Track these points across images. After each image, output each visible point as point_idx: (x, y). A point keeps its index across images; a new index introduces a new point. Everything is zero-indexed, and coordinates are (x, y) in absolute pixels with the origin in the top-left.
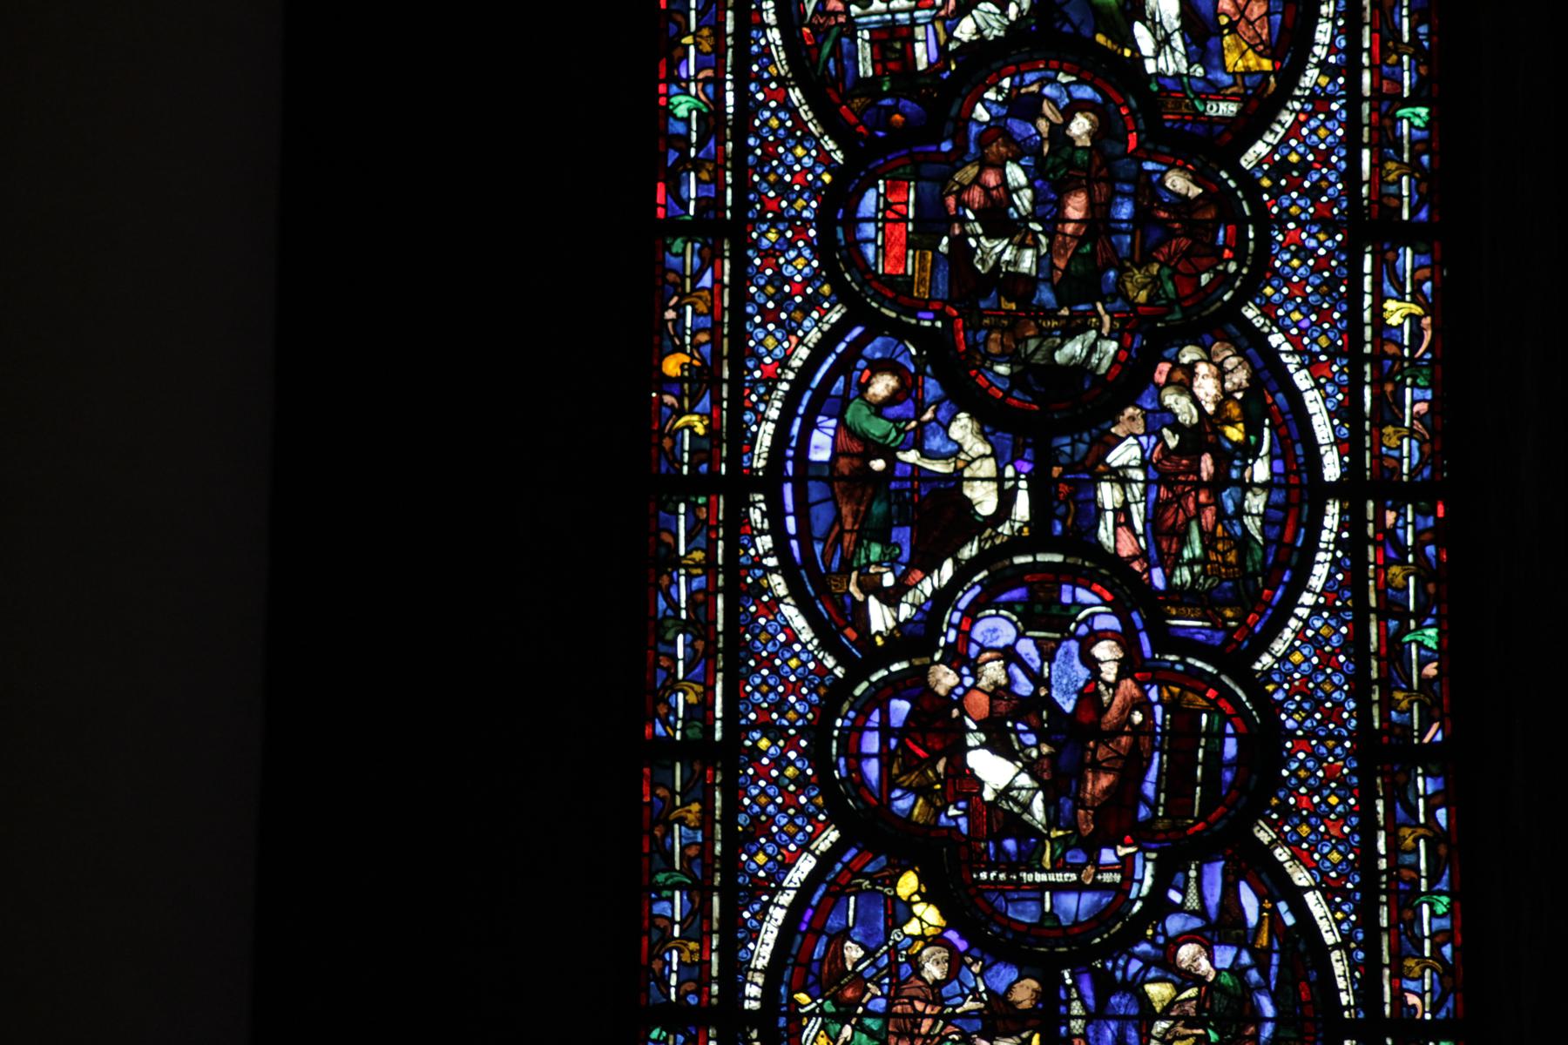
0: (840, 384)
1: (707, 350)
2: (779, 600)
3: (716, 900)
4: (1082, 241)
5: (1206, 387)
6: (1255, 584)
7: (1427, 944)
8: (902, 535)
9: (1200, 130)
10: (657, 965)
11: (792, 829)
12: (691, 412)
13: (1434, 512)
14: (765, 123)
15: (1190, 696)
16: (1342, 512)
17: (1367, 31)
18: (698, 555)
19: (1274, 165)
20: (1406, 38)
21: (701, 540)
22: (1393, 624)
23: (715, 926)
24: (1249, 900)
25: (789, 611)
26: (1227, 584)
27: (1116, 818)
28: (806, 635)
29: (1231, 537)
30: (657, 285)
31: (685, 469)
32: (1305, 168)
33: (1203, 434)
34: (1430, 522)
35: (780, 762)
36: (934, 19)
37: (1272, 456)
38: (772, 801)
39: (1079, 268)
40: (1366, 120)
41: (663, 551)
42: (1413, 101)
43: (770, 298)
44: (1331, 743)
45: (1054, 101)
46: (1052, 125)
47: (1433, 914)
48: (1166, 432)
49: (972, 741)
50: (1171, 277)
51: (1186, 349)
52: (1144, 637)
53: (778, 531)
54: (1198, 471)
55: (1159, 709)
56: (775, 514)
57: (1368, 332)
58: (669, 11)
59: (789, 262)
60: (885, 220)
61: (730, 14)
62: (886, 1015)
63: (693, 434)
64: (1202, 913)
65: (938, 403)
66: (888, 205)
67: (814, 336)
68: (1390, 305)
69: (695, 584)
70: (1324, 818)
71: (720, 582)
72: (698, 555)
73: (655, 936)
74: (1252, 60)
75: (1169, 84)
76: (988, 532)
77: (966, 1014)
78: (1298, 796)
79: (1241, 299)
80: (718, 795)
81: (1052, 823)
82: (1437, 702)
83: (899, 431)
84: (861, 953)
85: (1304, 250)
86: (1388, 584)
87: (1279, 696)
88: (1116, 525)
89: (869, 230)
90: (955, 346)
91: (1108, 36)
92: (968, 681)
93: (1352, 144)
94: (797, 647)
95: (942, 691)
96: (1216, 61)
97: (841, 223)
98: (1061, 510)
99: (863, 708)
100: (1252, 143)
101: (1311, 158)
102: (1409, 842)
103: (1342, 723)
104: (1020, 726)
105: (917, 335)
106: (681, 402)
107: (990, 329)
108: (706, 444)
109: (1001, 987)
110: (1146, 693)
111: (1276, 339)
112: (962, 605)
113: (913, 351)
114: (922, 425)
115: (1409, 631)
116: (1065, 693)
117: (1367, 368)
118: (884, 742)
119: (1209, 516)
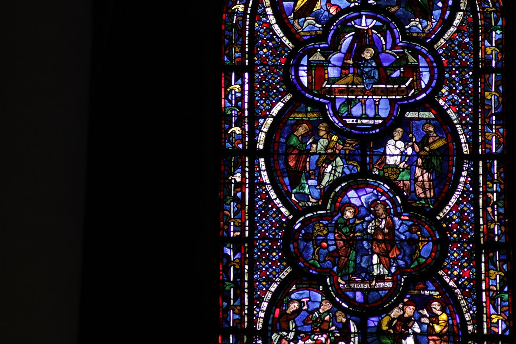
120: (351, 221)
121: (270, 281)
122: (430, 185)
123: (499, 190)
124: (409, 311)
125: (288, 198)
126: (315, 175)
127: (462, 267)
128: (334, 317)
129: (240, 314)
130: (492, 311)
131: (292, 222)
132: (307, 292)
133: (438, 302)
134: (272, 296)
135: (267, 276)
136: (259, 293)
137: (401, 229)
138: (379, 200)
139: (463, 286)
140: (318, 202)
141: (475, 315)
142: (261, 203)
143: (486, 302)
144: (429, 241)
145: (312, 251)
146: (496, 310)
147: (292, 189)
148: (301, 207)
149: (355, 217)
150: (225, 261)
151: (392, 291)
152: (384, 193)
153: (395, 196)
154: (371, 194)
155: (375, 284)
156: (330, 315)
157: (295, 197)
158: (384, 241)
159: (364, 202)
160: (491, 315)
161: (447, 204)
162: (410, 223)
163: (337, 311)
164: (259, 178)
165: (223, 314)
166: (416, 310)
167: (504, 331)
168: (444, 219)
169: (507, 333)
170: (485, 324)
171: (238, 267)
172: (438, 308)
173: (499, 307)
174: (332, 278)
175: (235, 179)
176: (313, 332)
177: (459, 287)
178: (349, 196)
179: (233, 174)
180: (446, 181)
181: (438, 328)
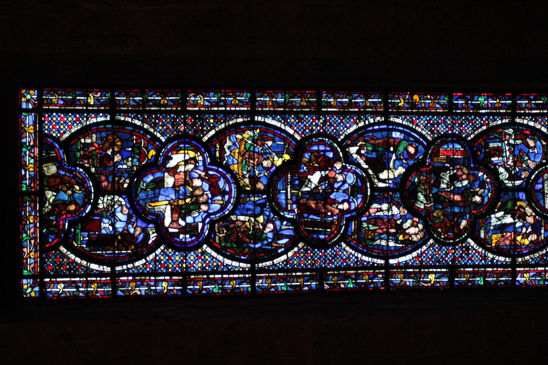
0: (412, 139)
1: (420, 106)
2: (357, 124)
3: (282, 109)
4: (449, 199)
5: (412, 230)
6: (363, 243)
7: (274, 285)
8: (374, 155)
9: (477, 228)
10: (266, 95)
11: (300, 128)
12: (404, 102)
13: (382, 287)
14: (477, 120)
15: (335, 227)
16: (381, 264)
17: (502, 269)
18: (368, 104)
19: (468, 247)
20: (500, 279)
21: (372, 105)
22: (354, 276)
23: (276, 109)
24: (284, 241)
25: (354, 127)
26: (363, 236)
27: (304, 209)
28: (349, 131)
29: (375, 237)
30: (436, 93)
31: (390, 101)
32: (468, 254)
33: (400, 229)
34: (379, 286)
35: (317, 125)
36: (504, 162)
37: (395, 247)
38: (307, 123)
39: (442, 198)
40: (480, 269)
41: (369, 95)
42: (485, 281)
43: (433, 122)
44: (324, 261)
45: (484, 192)
46: (478, 192)
47: (282, 286)
48: (401, 220)
49: (323, 173)
50: (440, 222)
51: (422, 226)
52: (349, 215)
53: (375, 124)
54: (391, 228)
55: (331, 219)
56: (379, 123)
57: (427, 270)
58: (505, 96)
59: (442, 126)
60: (453, 150)
61: (505, 111)
62: (254, 152)
63: (399, 103)
64: (281, 230)
65: (407, 164)
66: (457, 151)
67: (424, 133)
68: (434, 275)
69: (361, 104)
70: (305, 259)
71: (362, 110)
72: (368, 104)
73: (273, 94)
74: (494, 241)
75: (488, 221)
76: (375, 176)
77: (254, 171)
78: (310, 253)
79: (434, 239)
80: (308, 109)
81: (302, 192)
82: (334, 287)
83: (400, 154)
84: (269, 145)
85: (448, 255)
86: (364, 275)
87: (335, 249)
88: (377, 208)
89: (451, 146)
90: (422, 168)
91: (500, 205)
92: (338, 172)
93: (474, 266)
94: (345, 129)
95: (335, 165)
96: (494, 232)
97: (452, 139)
98: (381, 195)
99: (331, 146)
100: (474, 241)
101: (470, 256)
102: (299, 280)
103: (329, 264)
104: (326, 185)
105: (424, 159)
106: (407, 99)
107: (426, 177)
108: (396, 106)
109: (262, 180)
110: (335, 216)
111: (424, 248)
112: (357, 170)
113: (420, 157)
114: (402, 160)
115: (352, 280)
116: (335, 196)
117: (418, 270)
118: (322, 151)
119: (380, 231)
124: (530, 220)
128: (525, 170)
129: (526, 108)
130: (532, 274)
132: (541, 152)
146: (533, 276)
165: (526, 96)
166: (531, 224)
167: (518, 281)
169: (517, 283)
170: (523, 269)
172: (533, 239)
176: (514, 156)
181: (519, 238)
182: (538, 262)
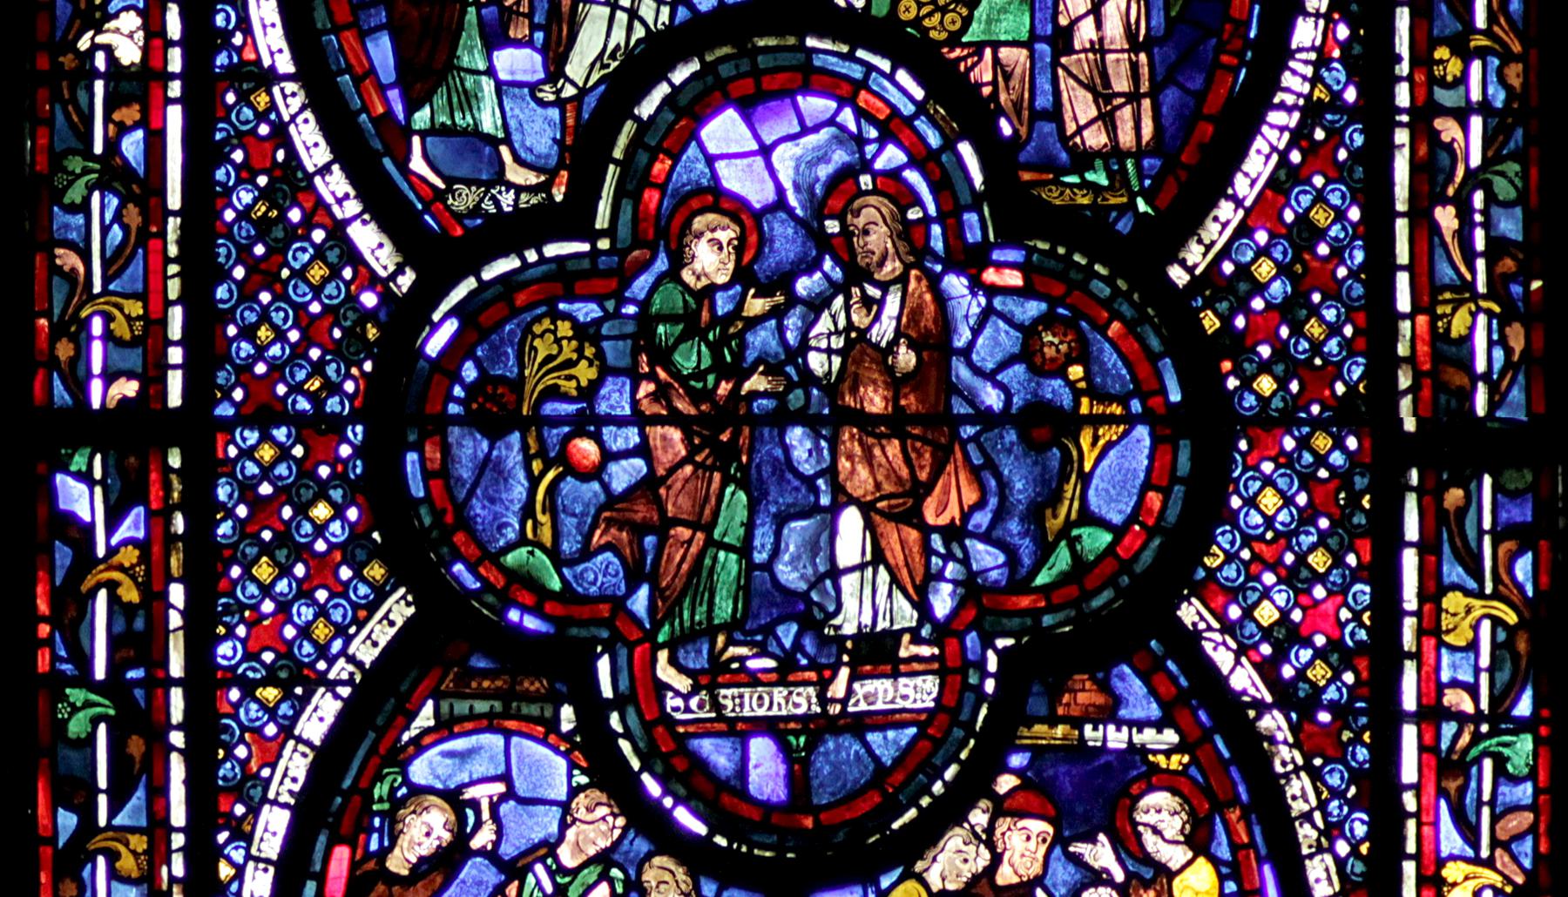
120: (723, 304)
121: (300, 680)
122: (1134, 67)
123: (1499, 98)
125: (387, 163)
126: (530, 16)
127: (1297, 578)
130: (1451, 840)
131: (408, 316)
132: (497, 741)
133: (1174, 792)
134: (312, 771)
135: (286, 651)
136: (241, 752)
137: (987, 352)
138: (866, 166)
139: (1303, 690)
140: (545, 187)
141: (1360, 868)
142: (247, 197)
143: (1417, 788)
144: (1130, 421)
145: (519, 490)
146: (1469, 832)
147: (411, 107)
148: (459, 217)
149: (743, 276)
150: (63, 555)
151: (935, 727)
152: (893, 127)
153: (949, 145)
154: (825, 133)
155: (850, 691)
156: (611, 882)
157: (426, 156)
158: (894, 424)
159: (788, 185)
160: (1441, 863)
161: (1219, 187)
162: (1034, 308)
163: (649, 857)
164: (238, 39)
166: (1060, 841)
168: (1208, 283)
171: (130, 594)
172: (1173, 826)
173: (1486, 811)
174: (623, 653)
175: (108, 49)
177: (1285, 696)
178: (713, 149)
179: (98, 18)
180: (1219, 50)
182: (1356, 776)
